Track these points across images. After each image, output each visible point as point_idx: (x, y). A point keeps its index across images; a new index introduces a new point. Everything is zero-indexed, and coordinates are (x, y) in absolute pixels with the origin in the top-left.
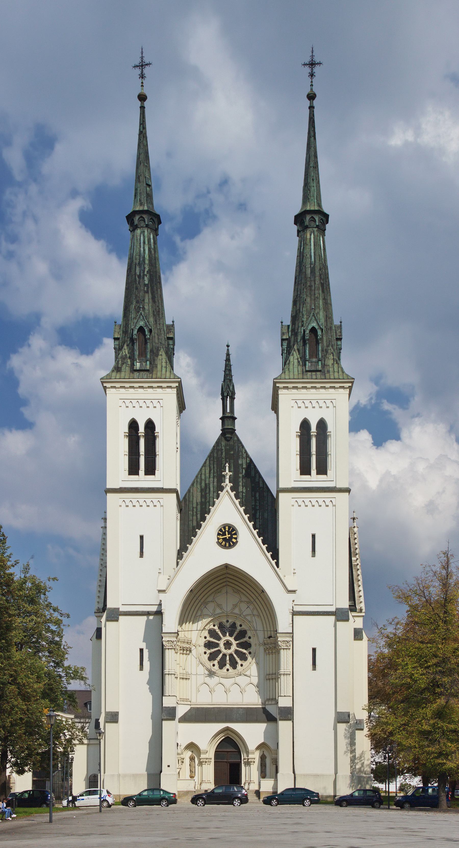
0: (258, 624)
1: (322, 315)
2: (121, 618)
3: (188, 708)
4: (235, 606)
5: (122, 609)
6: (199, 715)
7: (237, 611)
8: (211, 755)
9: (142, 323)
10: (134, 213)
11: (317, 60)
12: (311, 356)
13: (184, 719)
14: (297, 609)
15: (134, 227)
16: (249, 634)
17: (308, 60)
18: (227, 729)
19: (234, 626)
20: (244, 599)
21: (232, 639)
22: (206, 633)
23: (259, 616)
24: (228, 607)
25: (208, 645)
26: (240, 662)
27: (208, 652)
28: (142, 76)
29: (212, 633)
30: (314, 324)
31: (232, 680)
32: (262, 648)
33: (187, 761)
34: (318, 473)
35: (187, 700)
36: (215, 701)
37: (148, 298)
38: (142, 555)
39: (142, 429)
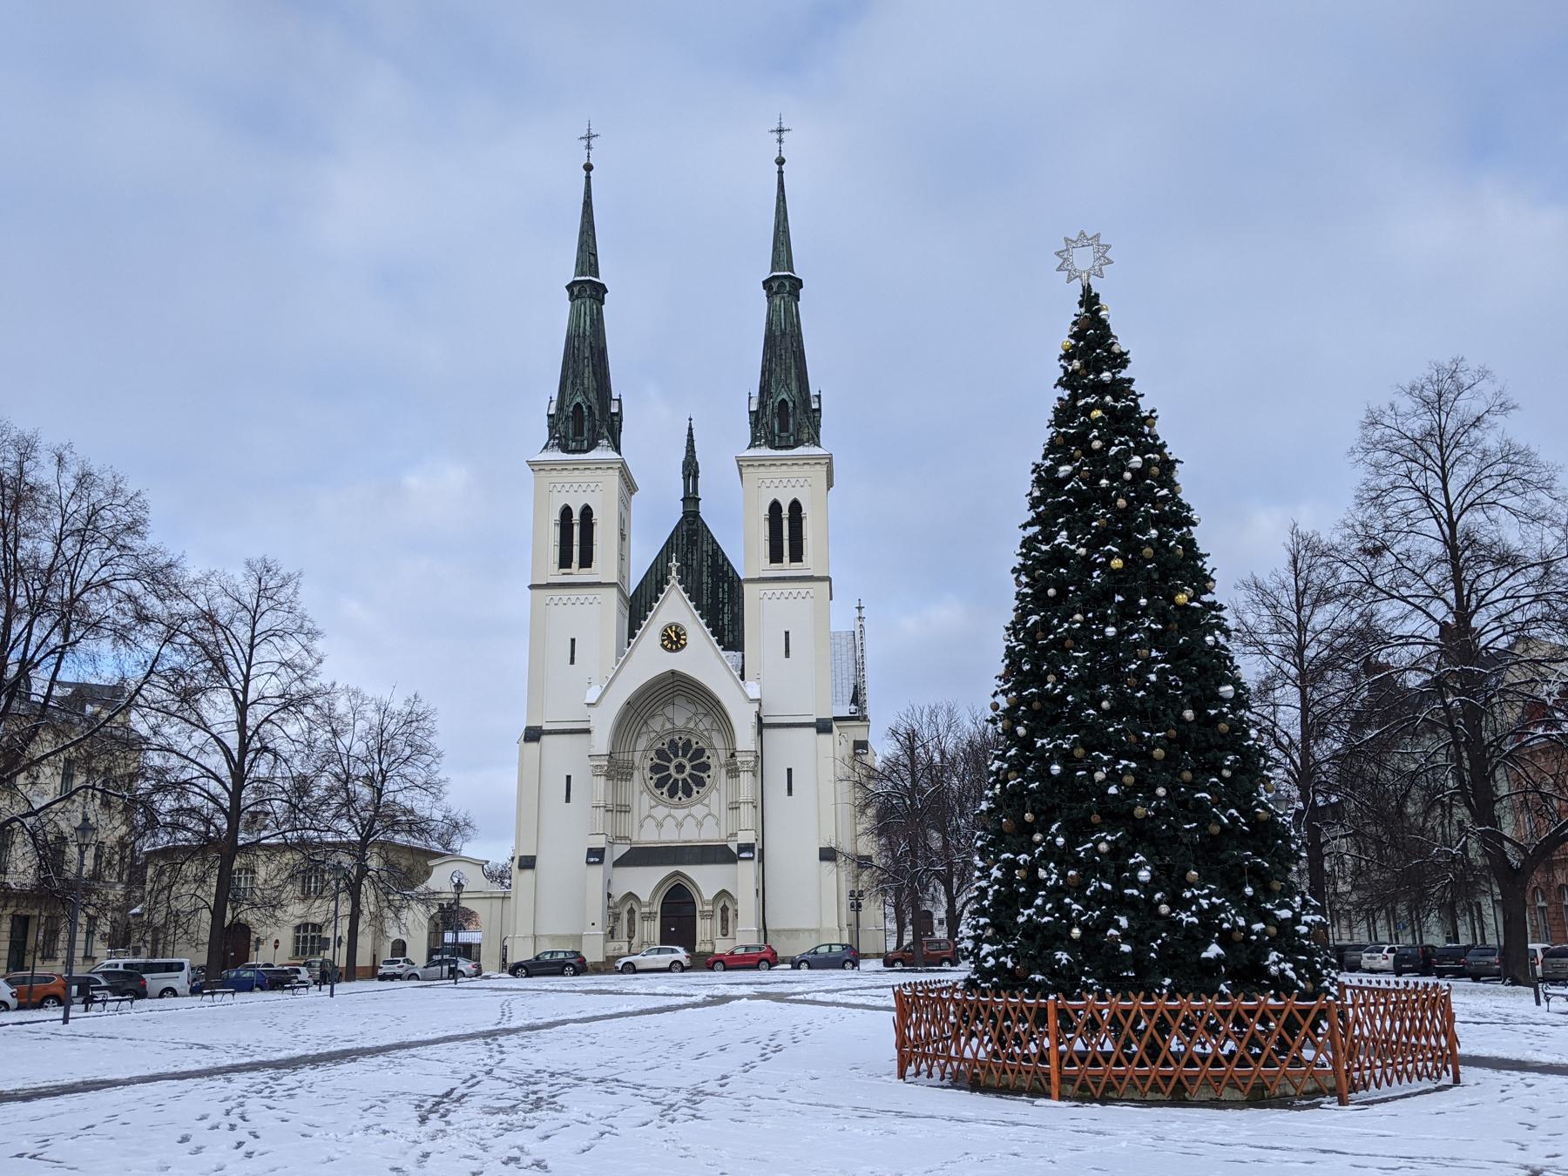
0: (718, 741)
1: (794, 385)
2: (544, 738)
3: (627, 848)
4: (690, 719)
5: (546, 727)
6: (640, 856)
7: (691, 725)
8: (657, 908)
9: (579, 400)
10: (575, 283)
11: (785, 126)
12: (781, 431)
13: (620, 863)
14: (766, 720)
15: (572, 298)
16: (707, 753)
17: (776, 127)
18: (678, 873)
19: (688, 744)
20: (701, 710)
21: (685, 761)
22: (653, 754)
23: (719, 731)
24: (680, 722)
25: (655, 769)
26: (695, 789)
27: (656, 777)
28: (589, 147)
29: (660, 754)
30: (785, 396)
31: (686, 811)
32: (724, 771)
33: (625, 916)
34: (791, 561)
35: (626, 838)
36: (663, 838)
37: (588, 372)
38: (572, 662)
39: (576, 517)
